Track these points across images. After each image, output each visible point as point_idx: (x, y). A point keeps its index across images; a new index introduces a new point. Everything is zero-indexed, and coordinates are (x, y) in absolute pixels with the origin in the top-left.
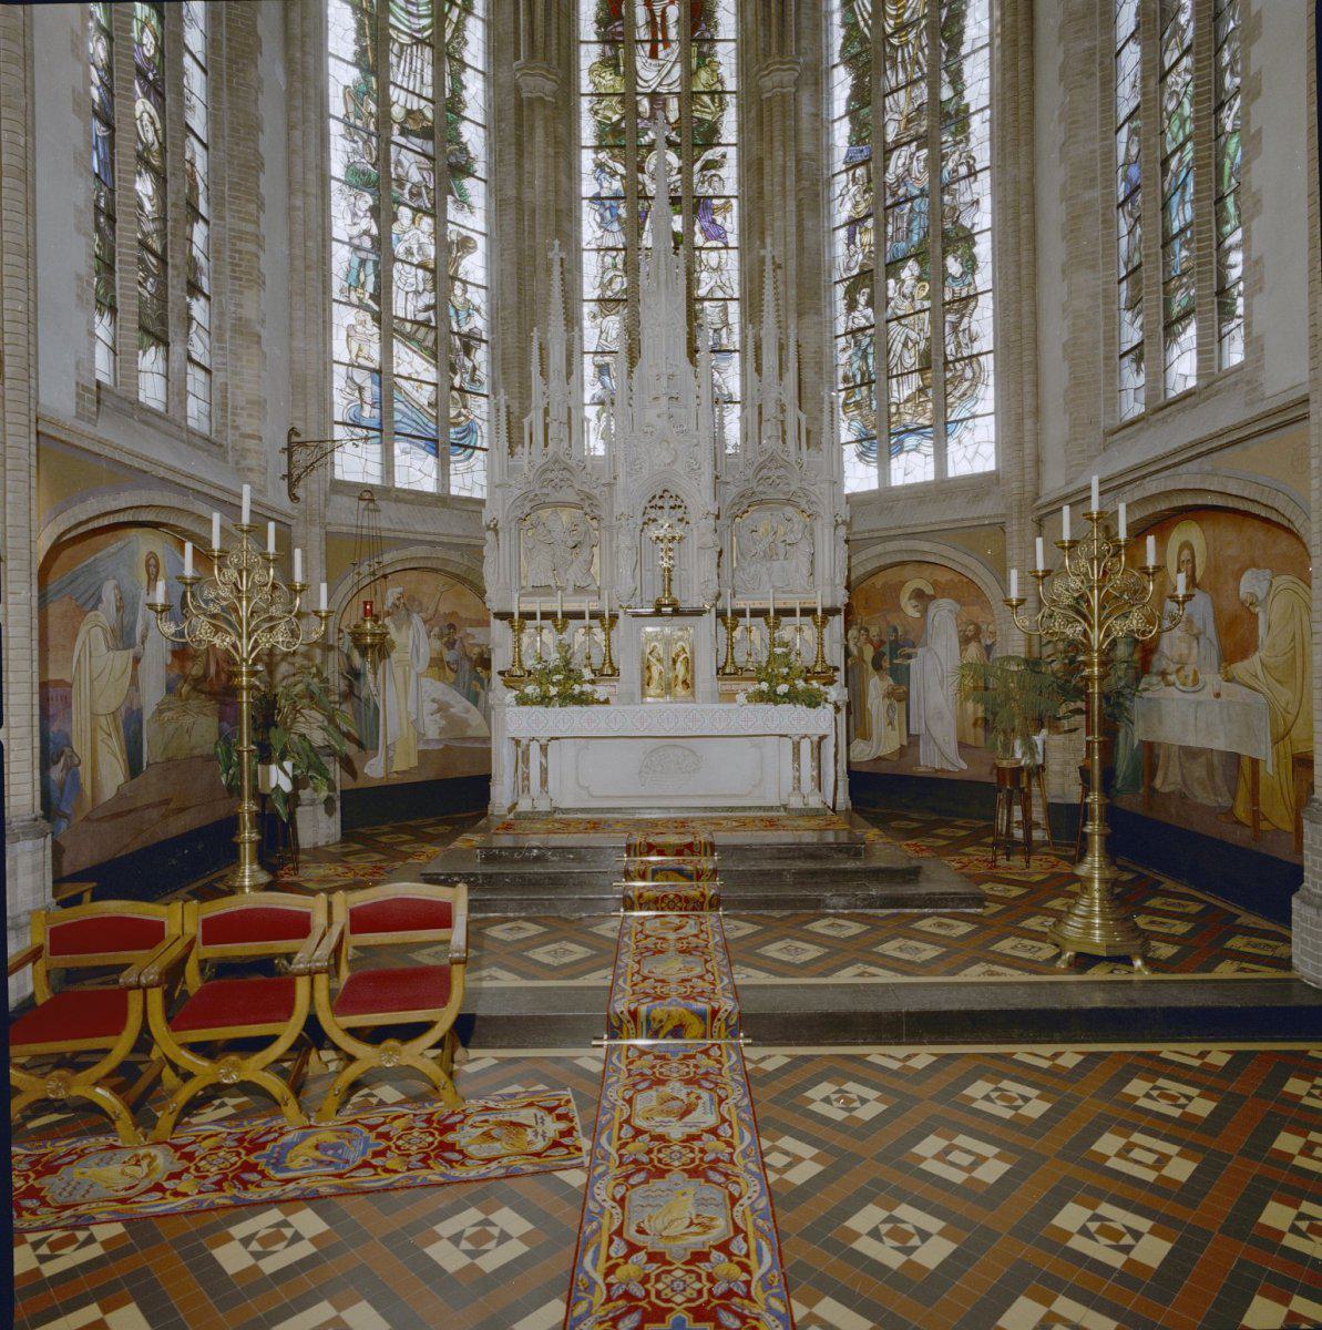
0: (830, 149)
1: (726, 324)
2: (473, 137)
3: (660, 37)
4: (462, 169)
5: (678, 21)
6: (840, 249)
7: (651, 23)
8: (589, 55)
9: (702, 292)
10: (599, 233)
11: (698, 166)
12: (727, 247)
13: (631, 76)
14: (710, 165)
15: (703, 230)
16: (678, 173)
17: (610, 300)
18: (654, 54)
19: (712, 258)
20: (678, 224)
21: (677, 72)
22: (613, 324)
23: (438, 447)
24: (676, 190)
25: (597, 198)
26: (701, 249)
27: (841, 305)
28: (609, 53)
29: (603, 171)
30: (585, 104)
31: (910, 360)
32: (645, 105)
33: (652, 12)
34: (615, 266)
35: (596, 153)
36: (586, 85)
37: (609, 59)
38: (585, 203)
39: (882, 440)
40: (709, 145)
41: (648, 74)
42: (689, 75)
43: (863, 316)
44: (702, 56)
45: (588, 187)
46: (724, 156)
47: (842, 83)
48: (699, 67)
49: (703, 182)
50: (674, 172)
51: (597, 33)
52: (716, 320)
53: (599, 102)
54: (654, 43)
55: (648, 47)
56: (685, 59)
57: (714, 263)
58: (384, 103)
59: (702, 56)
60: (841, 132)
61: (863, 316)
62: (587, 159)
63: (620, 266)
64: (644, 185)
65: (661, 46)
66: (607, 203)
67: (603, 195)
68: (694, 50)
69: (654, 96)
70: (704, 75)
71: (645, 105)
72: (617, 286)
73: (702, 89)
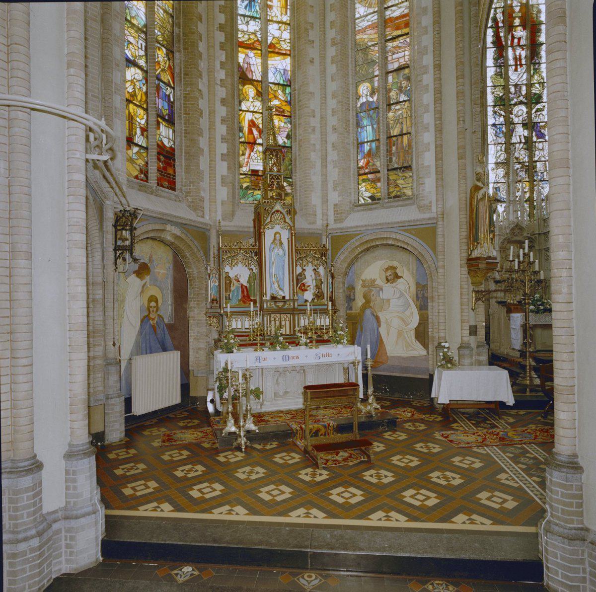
3: (518, 63)
5: (525, 57)
7: (515, 59)
9: (536, 159)
10: (495, 138)
11: (534, 111)
12: (546, 141)
15: (537, 135)
16: (527, 113)
17: (499, 163)
18: (516, 70)
19: (540, 146)
21: (525, 76)
22: (501, 172)
24: (525, 120)
26: (535, 142)
28: (498, 70)
29: (496, 114)
32: (512, 89)
33: (515, 54)
34: (501, 150)
35: (494, 108)
36: (489, 83)
37: (499, 72)
38: (489, 127)
40: (538, 102)
42: (531, 77)
46: (544, 106)
48: (534, 74)
49: (536, 117)
50: (524, 114)
51: (494, 63)
52: (542, 169)
53: (495, 89)
54: (516, 65)
55: (514, 67)
56: (528, 71)
57: (541, 147)
63: (503, 150)
64: (513, 119)
65: (519, 67)
66: (498, 126)
67: (496, 123)
68: (532, 68)
69: (516, 86)
70: (536, 77)
71: (512, 89)
72: (502, 158)
73: (535, 82)
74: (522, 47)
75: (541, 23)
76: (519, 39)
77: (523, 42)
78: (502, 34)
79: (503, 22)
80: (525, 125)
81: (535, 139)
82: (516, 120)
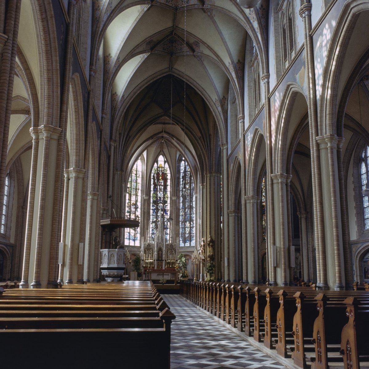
0: (180, 206)
1: (167, 225)
2: (139, 204)
4: (138, 208)
6: (181, 218)
8: (152, 193)
13: (157, 195)
14: (166, 206)
20: (162, 213)
22: (154, 224)
23: (134, 240)
25: (152, 209)
27: (181, 224)
30: (151, 198)
31: (188, 232)
39: (185, 242)
41: (159, 195)
43: (183, 226)
44: (166, 193)
45: (151, 208)
47: (181, 199)
58: (130, 203)
59: (166, 193)
60: (181, 204)
61: (183, 226)
62: (151, 205)
72: (154, 220)
74: (162, 186)
75: (168, 179)
76: (161, 183)
77: (162, 184)
78: (156, 181)
79: (156, 177)
80: (162, 210)
81: (165, 214)
82: (159, 208)
